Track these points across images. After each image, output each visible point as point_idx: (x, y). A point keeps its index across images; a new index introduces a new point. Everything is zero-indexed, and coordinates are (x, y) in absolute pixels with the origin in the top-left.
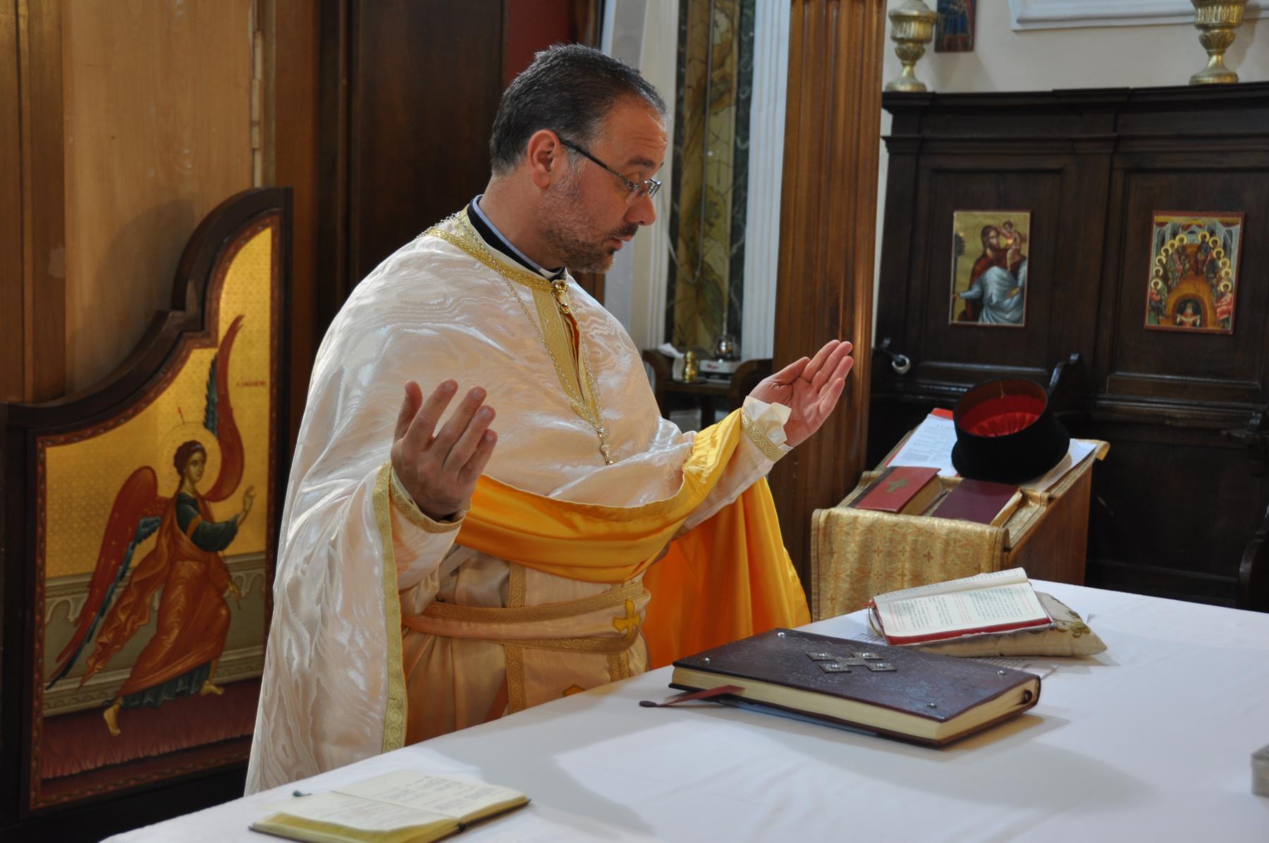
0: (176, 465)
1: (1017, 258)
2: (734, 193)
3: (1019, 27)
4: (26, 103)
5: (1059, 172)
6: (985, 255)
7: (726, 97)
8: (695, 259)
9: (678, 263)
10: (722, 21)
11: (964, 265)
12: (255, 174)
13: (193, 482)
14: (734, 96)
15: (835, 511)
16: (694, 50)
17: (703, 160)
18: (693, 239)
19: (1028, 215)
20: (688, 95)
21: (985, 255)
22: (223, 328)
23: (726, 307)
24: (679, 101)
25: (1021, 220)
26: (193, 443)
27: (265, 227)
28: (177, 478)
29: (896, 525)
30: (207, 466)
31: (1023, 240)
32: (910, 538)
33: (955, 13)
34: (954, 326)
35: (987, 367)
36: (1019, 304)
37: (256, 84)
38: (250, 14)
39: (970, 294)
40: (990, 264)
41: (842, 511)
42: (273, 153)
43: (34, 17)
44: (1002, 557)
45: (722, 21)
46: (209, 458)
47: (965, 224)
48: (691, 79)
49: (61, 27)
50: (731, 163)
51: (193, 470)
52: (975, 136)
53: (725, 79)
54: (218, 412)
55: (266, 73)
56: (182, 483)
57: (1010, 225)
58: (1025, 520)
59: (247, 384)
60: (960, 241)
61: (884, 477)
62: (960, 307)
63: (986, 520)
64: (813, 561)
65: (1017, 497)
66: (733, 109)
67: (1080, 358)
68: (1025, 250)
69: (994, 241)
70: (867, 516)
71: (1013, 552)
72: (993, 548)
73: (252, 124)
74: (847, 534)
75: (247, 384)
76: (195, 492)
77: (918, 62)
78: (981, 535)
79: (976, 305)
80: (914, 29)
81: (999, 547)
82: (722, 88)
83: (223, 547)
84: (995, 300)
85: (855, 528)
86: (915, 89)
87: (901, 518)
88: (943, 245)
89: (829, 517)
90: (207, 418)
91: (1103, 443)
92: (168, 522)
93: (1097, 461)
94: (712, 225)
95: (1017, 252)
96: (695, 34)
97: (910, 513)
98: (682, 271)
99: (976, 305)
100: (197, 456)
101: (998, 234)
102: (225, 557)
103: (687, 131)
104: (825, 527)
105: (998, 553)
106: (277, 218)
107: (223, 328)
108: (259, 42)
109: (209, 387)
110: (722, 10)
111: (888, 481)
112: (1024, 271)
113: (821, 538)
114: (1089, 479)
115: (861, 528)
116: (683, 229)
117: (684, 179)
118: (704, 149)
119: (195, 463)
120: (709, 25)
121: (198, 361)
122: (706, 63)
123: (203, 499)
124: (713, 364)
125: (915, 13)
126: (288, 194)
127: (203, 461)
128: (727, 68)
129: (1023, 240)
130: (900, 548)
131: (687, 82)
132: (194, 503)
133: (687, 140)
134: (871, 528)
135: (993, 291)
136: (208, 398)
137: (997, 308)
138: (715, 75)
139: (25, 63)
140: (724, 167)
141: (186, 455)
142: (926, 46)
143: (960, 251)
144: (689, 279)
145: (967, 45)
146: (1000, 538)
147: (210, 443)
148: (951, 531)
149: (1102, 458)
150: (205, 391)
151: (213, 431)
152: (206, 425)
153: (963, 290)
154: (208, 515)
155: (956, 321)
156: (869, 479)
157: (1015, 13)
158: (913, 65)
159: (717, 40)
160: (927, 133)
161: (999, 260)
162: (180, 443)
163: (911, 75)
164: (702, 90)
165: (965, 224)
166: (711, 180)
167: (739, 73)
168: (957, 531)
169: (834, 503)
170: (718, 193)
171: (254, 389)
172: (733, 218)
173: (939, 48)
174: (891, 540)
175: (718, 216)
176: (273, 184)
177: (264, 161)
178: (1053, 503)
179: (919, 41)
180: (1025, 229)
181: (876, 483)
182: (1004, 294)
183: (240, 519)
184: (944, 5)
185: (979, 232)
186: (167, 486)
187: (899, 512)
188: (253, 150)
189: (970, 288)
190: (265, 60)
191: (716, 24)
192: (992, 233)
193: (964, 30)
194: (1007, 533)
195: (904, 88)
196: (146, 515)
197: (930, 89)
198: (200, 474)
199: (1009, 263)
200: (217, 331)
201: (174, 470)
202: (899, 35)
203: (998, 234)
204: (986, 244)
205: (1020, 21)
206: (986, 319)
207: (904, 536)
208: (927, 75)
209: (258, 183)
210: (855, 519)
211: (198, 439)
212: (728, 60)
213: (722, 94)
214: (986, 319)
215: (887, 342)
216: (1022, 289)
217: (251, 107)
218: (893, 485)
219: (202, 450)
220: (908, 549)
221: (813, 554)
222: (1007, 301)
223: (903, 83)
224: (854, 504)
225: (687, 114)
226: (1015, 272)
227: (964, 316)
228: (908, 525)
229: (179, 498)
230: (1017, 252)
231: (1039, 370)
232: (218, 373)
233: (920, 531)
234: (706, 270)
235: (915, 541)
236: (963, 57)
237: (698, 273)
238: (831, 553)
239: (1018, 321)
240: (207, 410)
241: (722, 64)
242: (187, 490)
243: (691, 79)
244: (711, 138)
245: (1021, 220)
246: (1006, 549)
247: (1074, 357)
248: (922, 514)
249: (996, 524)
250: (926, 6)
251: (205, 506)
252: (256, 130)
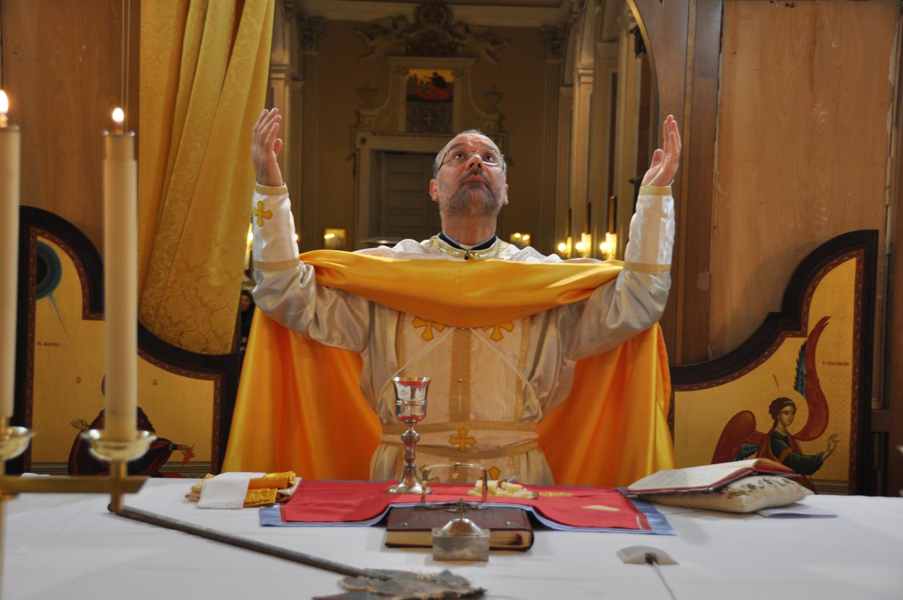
0: (770, 412)
13: (785, 426)
22: (811, 326)
26: (785, 399)
27: (851, 257)
28: (773, 421)
30: (796, 415)
37: (889, 160)
38: (889, 113)
51: (785, 417)
54: (807, 379)
56: (775, 425)
73: (885, 188)
76: (786, 432)
83: (811, 473)
90: (797, 384)
92: (764, 449)
100: (788, 408)
102: (812, 480)
106: (862, 251)
107: (811, 326)
109: (799, 363)
119: (787, 413)
121: (791, 347)
123: (793, 438)
127: (794, 412)
132: (786, 439)
136: (798, 370)
141: (778, 406)
150: (795, 365)
154: (797, 449)
183: (824, 456)
186: (764, 425)
188: (887, 206)
196: (747, 442)
198: (791, 421)
200: (806, 325)
201: (770, 416)
217: (886, 176)
219: (793, 405)
229: (773, 434)
232: (807, 355)
240: (797, 379)
242: (780, 429)
251: (795, 443)
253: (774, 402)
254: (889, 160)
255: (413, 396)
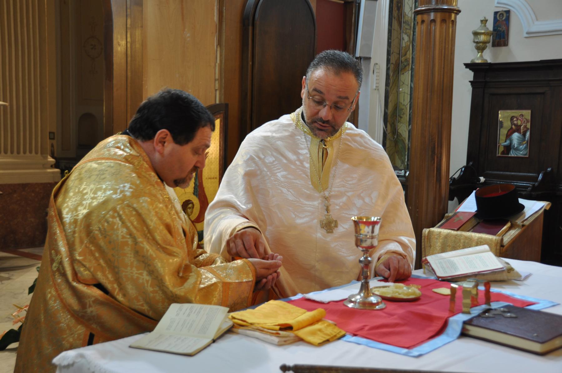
1: (525, 129)
2: (410, 105)
3: (527, 36)
4: (129, 74)
5: (543, 93)
6: (512, 128)
7: (407, 67)
8: (395, 131)
9: (387, 133)
10: (406, 38)
11: (503, 132)
12: (217, 99)
14: (410, 67)
15: (432, 229)
16: (394, 49)
17: (398, 93)
18: (393, 123)
19: (530, 111)
20: (392, 67)
21: (512, 128)
23: (407, 150)
24: (388, 69)
25: (527, 114)
29: (456, 235)
31: (528, 121)
32: (462, 241)
33: (500, 31)
34: (499, 157)
35: (513, 173)
36: (526, 148)
37: (217, 65)
39: (505, 144)
40: (514, 132)
41: (435, 230)
42: (223, 90)
43: (133, 42)
44: (500, 250)
45: (406, 38)
46: (195, 206)
47: (503, 115)
48: (393, 60)
49: (144, 44)
50: (409, 93)
51: (189, 211)
52: (508, 80)
53: (407, 60)
55: (221, 61)
57: (522, 115)
58: (512, 234)
59: (210, 178)
60: (501, 122)
61: (455, 214)
62: (501, 149)
63: (494, 234)
64: (423, 249)
65: (509, 224)
66: (410, 72)
67: (552, 170)
68: (529, 126)
69: (515, 122)
70: (445, 231)
71: (505, 248)
72: (496, 245)
73: (215, 80)
74: (437, 239)
75: (210, 178)
77: (484, 51)
78: (491, 240)
79: (508, 148)
80: (482, 38)
81: (499, 245)
82: (406, 64)
84: (516, 146)
85: (440, 236)
86: (483, 62)
87: (459, 233)
88: (495, 124)
89: (429, 231)
91: (548, 203)
93: (545, 210)
94: (401, 117)
95: (525, 127)
96: (395, 43)
97: (463, 230)
98: (389, 136)
99: (508, 148)
100: (190, 205)
101: (517, 119)
103: (391, 81)
104: (428, 236)
105: (498, 247)
106: (222, 115)
108: (219, 49)
110: (406, 33)
111: (455, 218)
112: (528, 134)
113: (426, 240)
114: (542, 217)
115: (442, 236)
116: (389, 119)
117: (389, 100)
118: (398, 88)
120: (400, 39)
122: (399, 54)
124: (400, 172)
125: (483, 31)
126: (227, 105)
127: (193, 208)
128: (408, 56)
129: (528, 121)
130: (458, 245)
131: (391, 62)
133: (391, 84)
134: (447, 236)
135: (515, 142)
137: (517, 149)
138: (403, 59)
139: (129, 59)
140: (406, 95)
142: (487, 45)
143: (502, 127)
144: (392, 139)
145: (506, 44)
146: (499, 241)
147: (196, 200)
148: (479, 238)
149: (548, 208)
151: (197, 196)
152: (194, 194)
153: (502, 142)
155: (499, 155)
156: (448, 217)
157: (525, 31)
158: (482, 52)
159: (404, 45)
160: (488, 79)
161: (518, 130)
162: (184, 201)
163: (481, 56)
164: (397, 65)
165: (503, 115)
166: (401, 100)
167: (412, 58)
168: (481, 238)
169: (433, 226)
170: (404, 105)
171: (213, 180)
172: (410, 114)
173: (494, 45)
174: (455, 242)
175: (404, 114)
176: (223, 102)
177: (220, 94)
178: (524, 228)
179: (485, 43)
180: (529, 118)
181: (450, 218)
182: (520, 144)
184: (496, 28)
185: (509, 118)
187: (458, 230)
188: (216, 90)
189: (505, 142)
190: (221, 56)
191: (403, 39)
192: (515, 119)
193: (504, 38)
194: (502, 240)
195: (479, 61)
197: (489, 61)
198: (192, 212)
199: (522, 131)
202: (476, 41)
203: (517, 119)
204: (512, 123)
205: (527, 33)
206: (512, 154)
207: (460, 240)
208: (489, 56)
209: (218, 102)
210: (440, 232)
211: (191, 199)
212: (408, 52)
213: (406, 66)
214: (512, 154)
215: (471, 163)
216: (527, 142)
217: (215, 74)
218: (456, 219)
219: (192, 203)
220: (461, 245)
221: (423, 247)
222: (521, 147)
223: (478, 59)
224: (440, 227)
225: (391, 74)
226: (524, 135)
227: (503, 153)
228: (461, 235)
230: (525, 127)
231: (534, 175)
233: (466, 238)
234: (399, 135)
235: (464, 242)
236: (504, 48)
237: (396, 137)
238: (430, 246)
239: (525, 155)
240: (194, 188)
241: (406, 54)
243: (393, 60)
244: (401, 83)
245: (527, 114)
246: (502, 246)
247: (549, 169)
248: (468, 231)
249: (499, 236)
250: (488, 29)
252: (217, 82)
253: (184, 203)
254: (217, 65)
255: (373, 232)
